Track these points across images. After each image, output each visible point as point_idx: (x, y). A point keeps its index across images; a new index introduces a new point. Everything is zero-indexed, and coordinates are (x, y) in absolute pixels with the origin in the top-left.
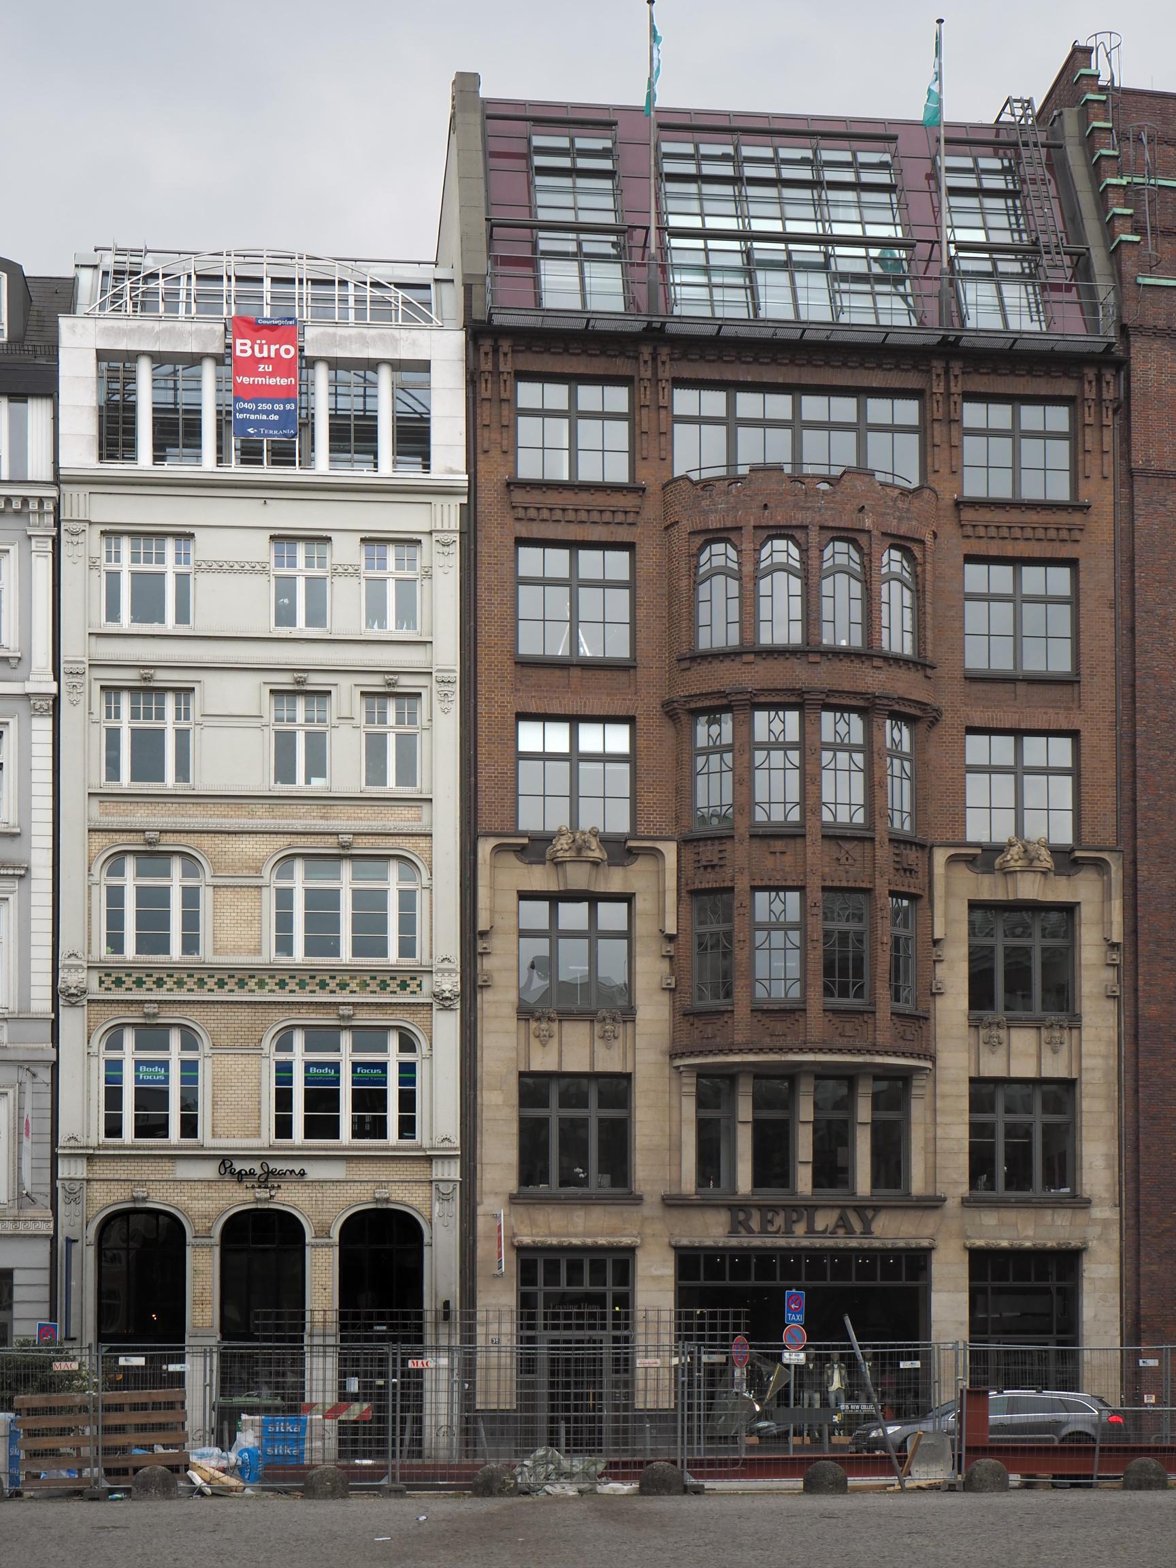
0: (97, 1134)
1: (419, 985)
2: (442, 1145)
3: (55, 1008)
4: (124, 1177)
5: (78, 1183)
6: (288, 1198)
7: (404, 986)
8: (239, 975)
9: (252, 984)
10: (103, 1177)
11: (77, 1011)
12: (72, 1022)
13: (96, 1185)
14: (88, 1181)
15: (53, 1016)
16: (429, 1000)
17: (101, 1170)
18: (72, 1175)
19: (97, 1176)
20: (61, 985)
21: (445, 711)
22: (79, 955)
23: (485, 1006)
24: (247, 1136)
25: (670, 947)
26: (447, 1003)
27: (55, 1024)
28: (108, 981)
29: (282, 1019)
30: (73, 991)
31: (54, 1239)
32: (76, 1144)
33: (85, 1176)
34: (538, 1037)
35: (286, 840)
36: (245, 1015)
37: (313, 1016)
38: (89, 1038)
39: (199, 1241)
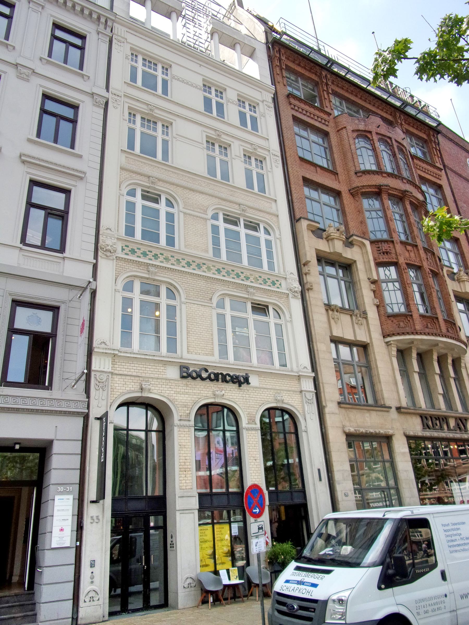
0: (117, 343)
1: (280, 285)
2: (304, 370)
3: (96, 257)
4: (134, 374)
5: (106, 375)
6: (229, 395)
7: (274, 283)
8: (198, 261)
9: (204, 267)
10: (121, 372)
11: (110, 262)
12: (105, 266)
13: (116, 378)
14: (112, 373)
15: (95, 261)
16: (287, 292)
17: (122, 368)
18: (102, 369)
19: (116, 372)
20: (101, 243)
21: (277, 167)
22: (113, 229)
23: (311, 299)
24: (207, 355)
25: (373, 286)
26: (296, 294)
27: (95, 267)
28: (127, 250)
29: (221, 290)
30: (109, 248)
31: (86, 417)
32: (105, 347)
33: (110, 370)
34: (333, 319)
35: (217, 200)
36: (202, 284)
37: (235, 290)
38: (116, 280)
39: (182, 423)
